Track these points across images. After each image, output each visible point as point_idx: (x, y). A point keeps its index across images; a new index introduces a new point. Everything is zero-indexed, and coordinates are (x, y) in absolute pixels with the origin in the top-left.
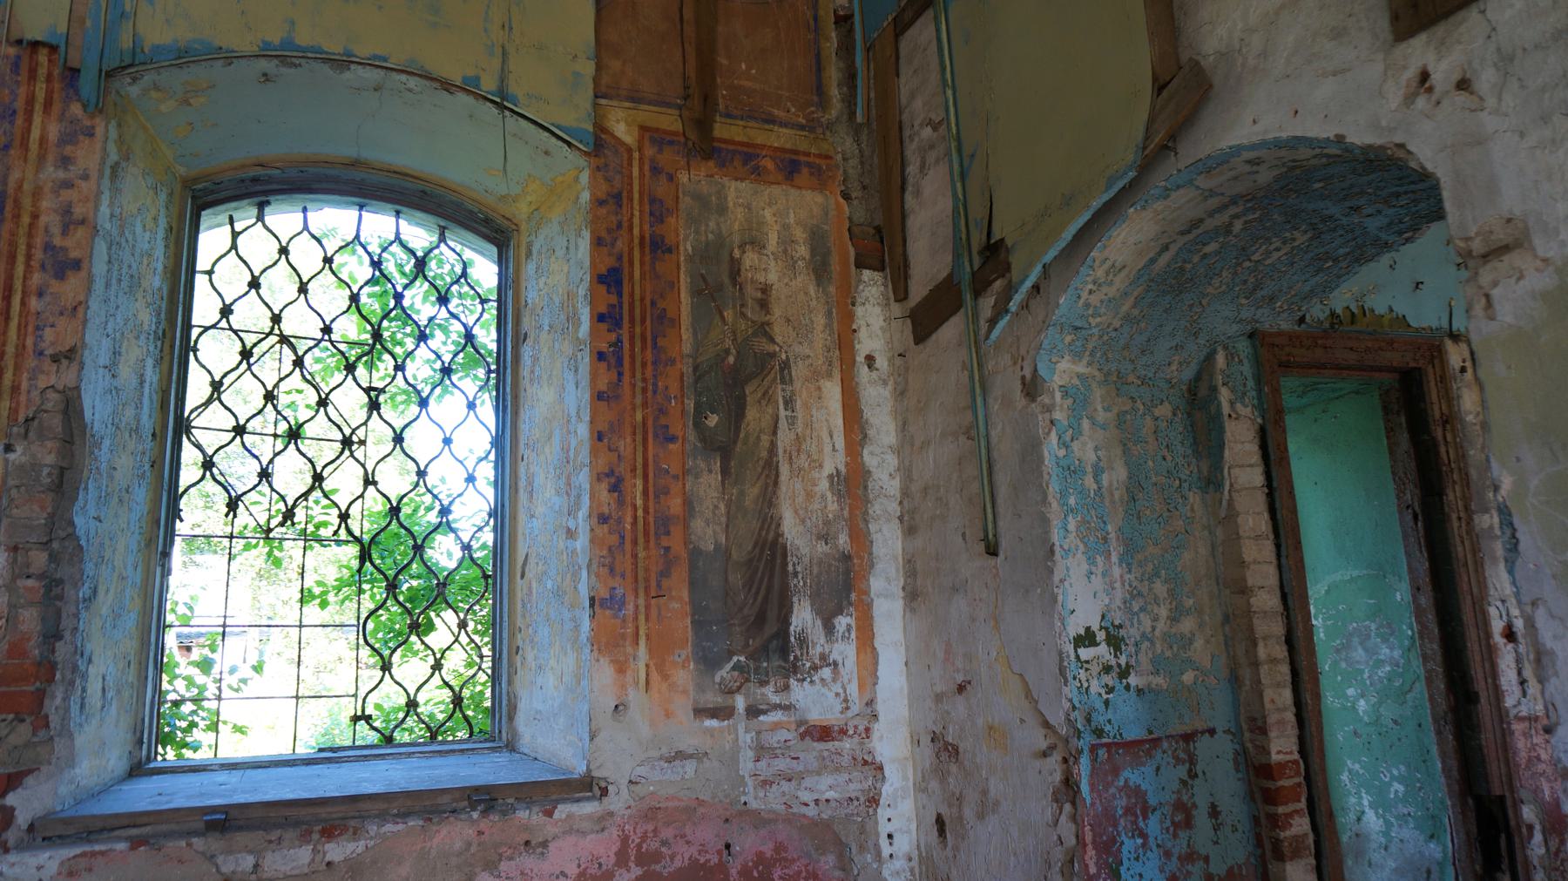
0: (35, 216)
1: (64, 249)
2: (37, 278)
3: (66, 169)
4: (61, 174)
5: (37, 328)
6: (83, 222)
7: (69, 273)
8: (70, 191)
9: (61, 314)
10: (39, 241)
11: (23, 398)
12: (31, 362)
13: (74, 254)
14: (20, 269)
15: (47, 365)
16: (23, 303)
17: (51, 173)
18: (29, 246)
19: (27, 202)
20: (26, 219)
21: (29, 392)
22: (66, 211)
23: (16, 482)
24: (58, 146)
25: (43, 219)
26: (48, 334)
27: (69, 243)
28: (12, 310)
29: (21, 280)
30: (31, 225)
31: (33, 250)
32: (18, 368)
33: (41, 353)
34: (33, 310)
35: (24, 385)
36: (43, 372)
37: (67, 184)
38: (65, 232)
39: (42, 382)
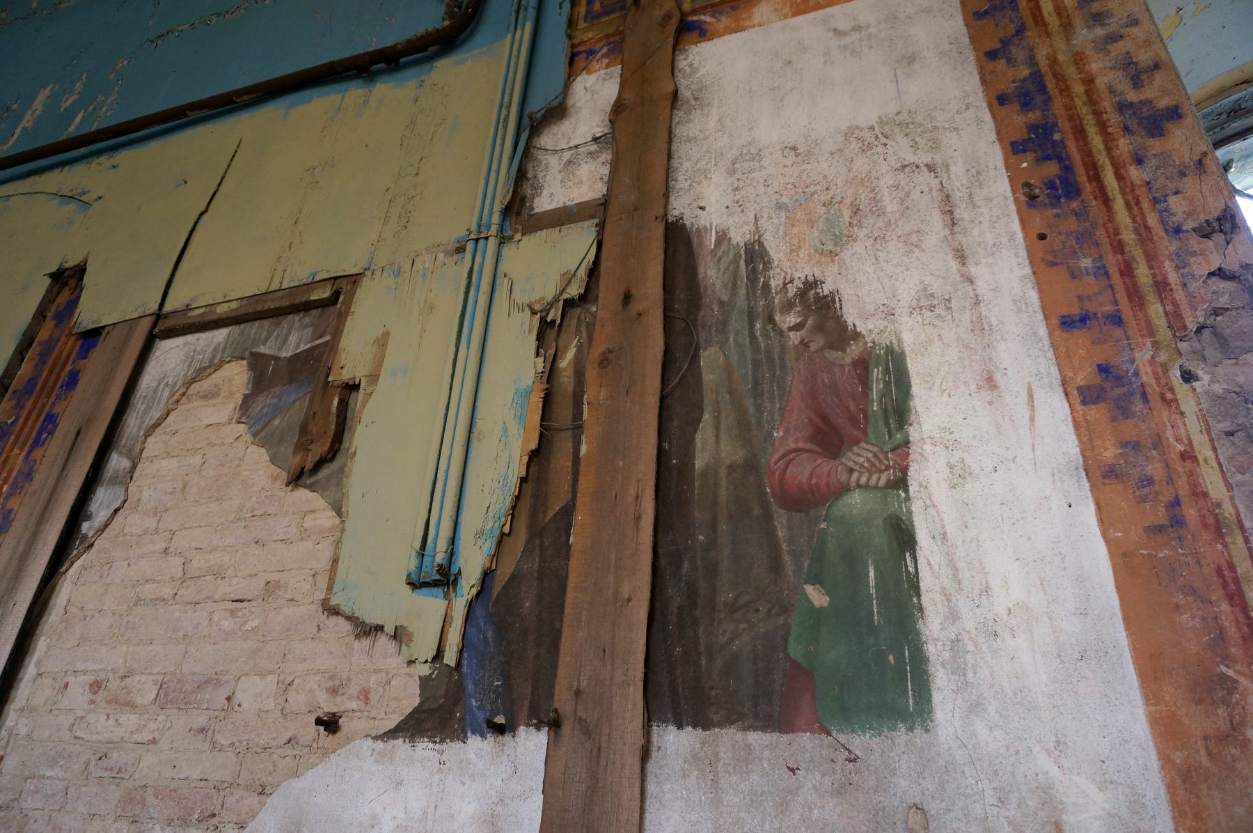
0: (1089, 81)
1: (1148, 102)
2: (1124, 145)
3: (1103, 25)
4: (1100, 32)
5: (1156, 201)
6: (1157, 66)
7: (1168, 125)
8: (1121, 43)
9: (1183, 174)
10: (1106, 104)
11: (1180, 295)
12: (1168, 246)
13: (1164, 103)
14: (1096, 141)
15: (1195, 242)
16: (1120, 177)
17: (1084, 36)
18: (1098, 114)
19: (1071, 71)
20: (1078, 89)
21: (1185, 285)
22: (1128, 63)
23: (1226, 425)
24: (1081, 7)
25: (1101, 82)
26: (1176, 204)
27: (1148, 93)
28: (1109, 190)
29: (1104, 153)
30: (1088, 93)
31: (1105, 116)
32: (1151, 258)
33: (1178, 230)
34: (1137, 182)
35: (1173, 278)
36: (1194, 254)
37: (1115, 38)
38: (1137, 83)
39: (1201, 267)
